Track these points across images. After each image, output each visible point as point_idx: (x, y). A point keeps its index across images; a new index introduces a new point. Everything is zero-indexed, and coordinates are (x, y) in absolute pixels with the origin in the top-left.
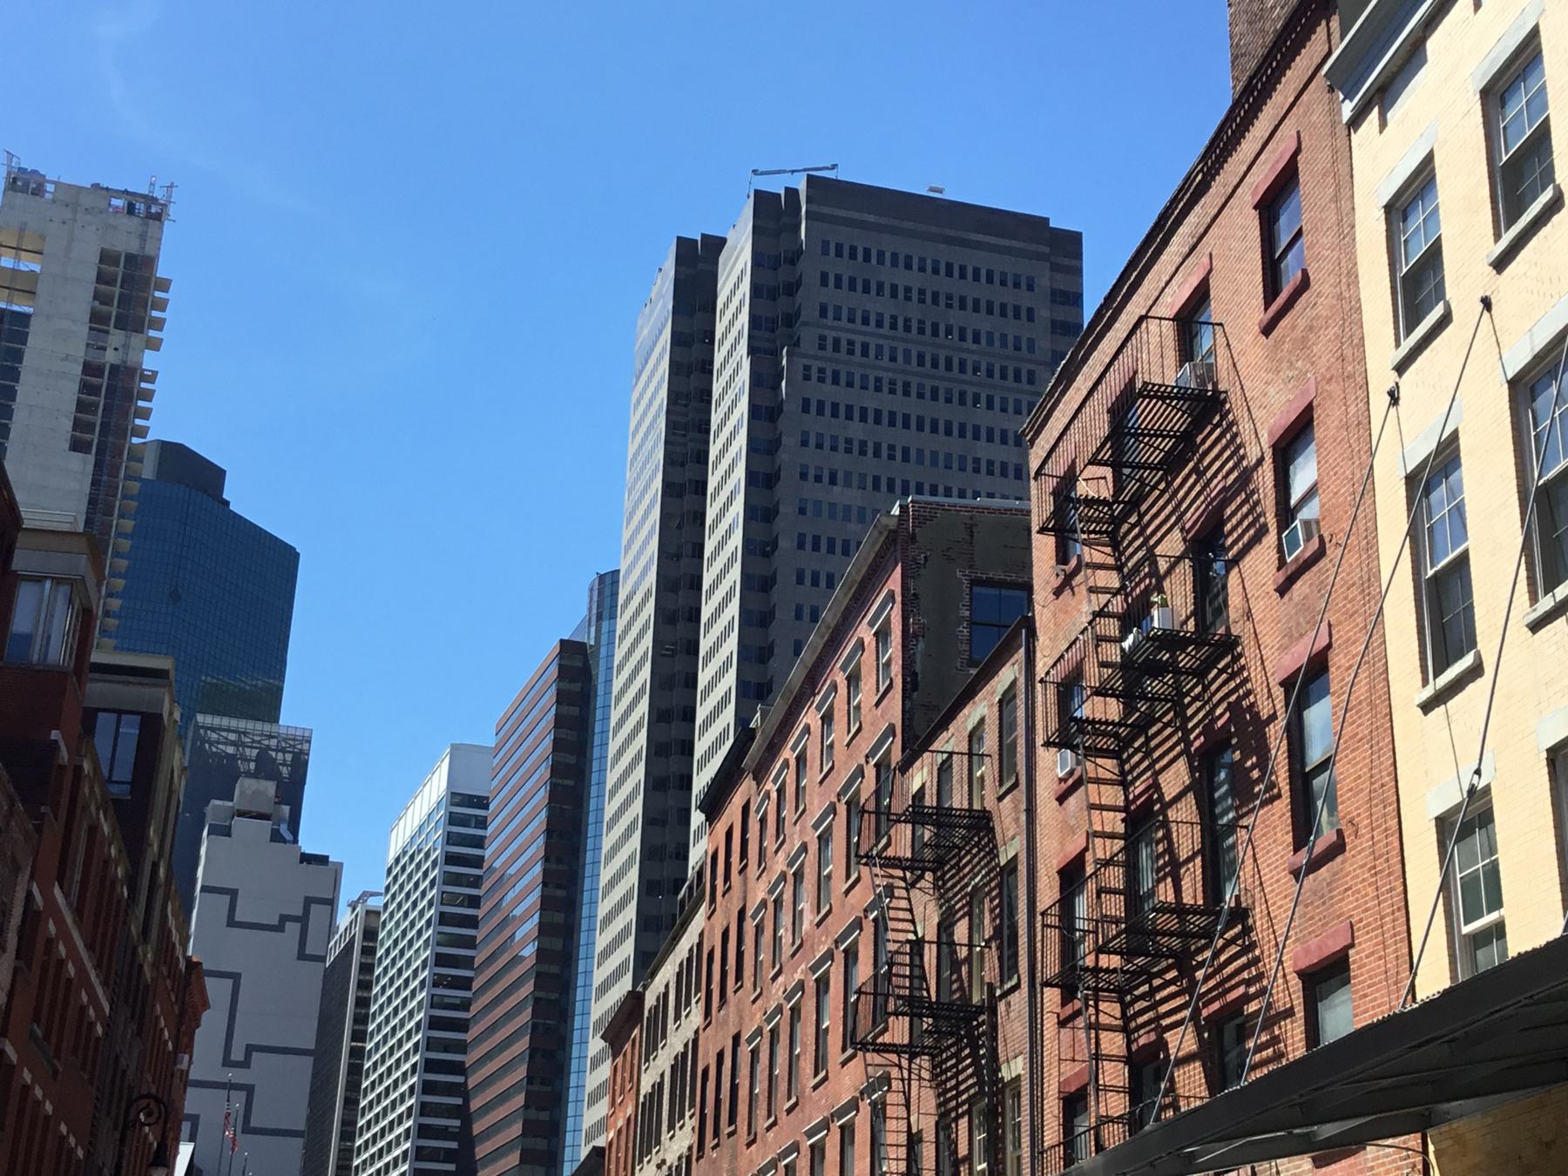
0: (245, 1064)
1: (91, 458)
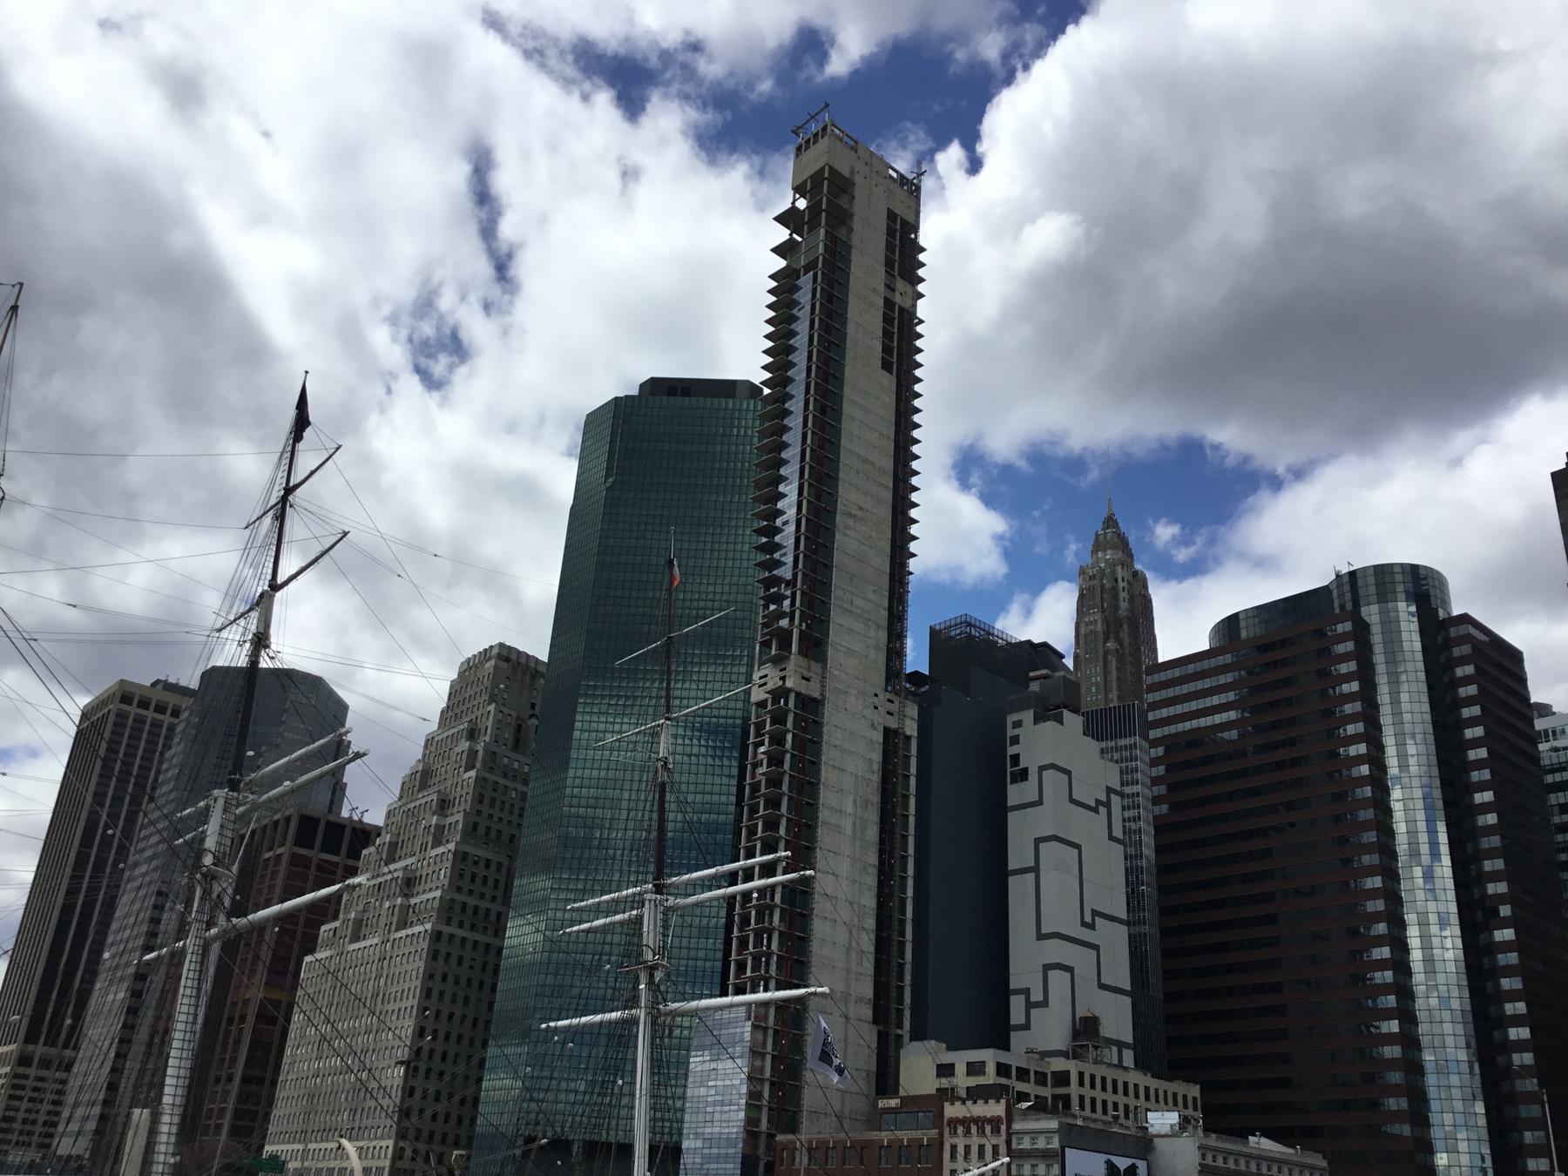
0: (1092, 926)
1: (895, 380)
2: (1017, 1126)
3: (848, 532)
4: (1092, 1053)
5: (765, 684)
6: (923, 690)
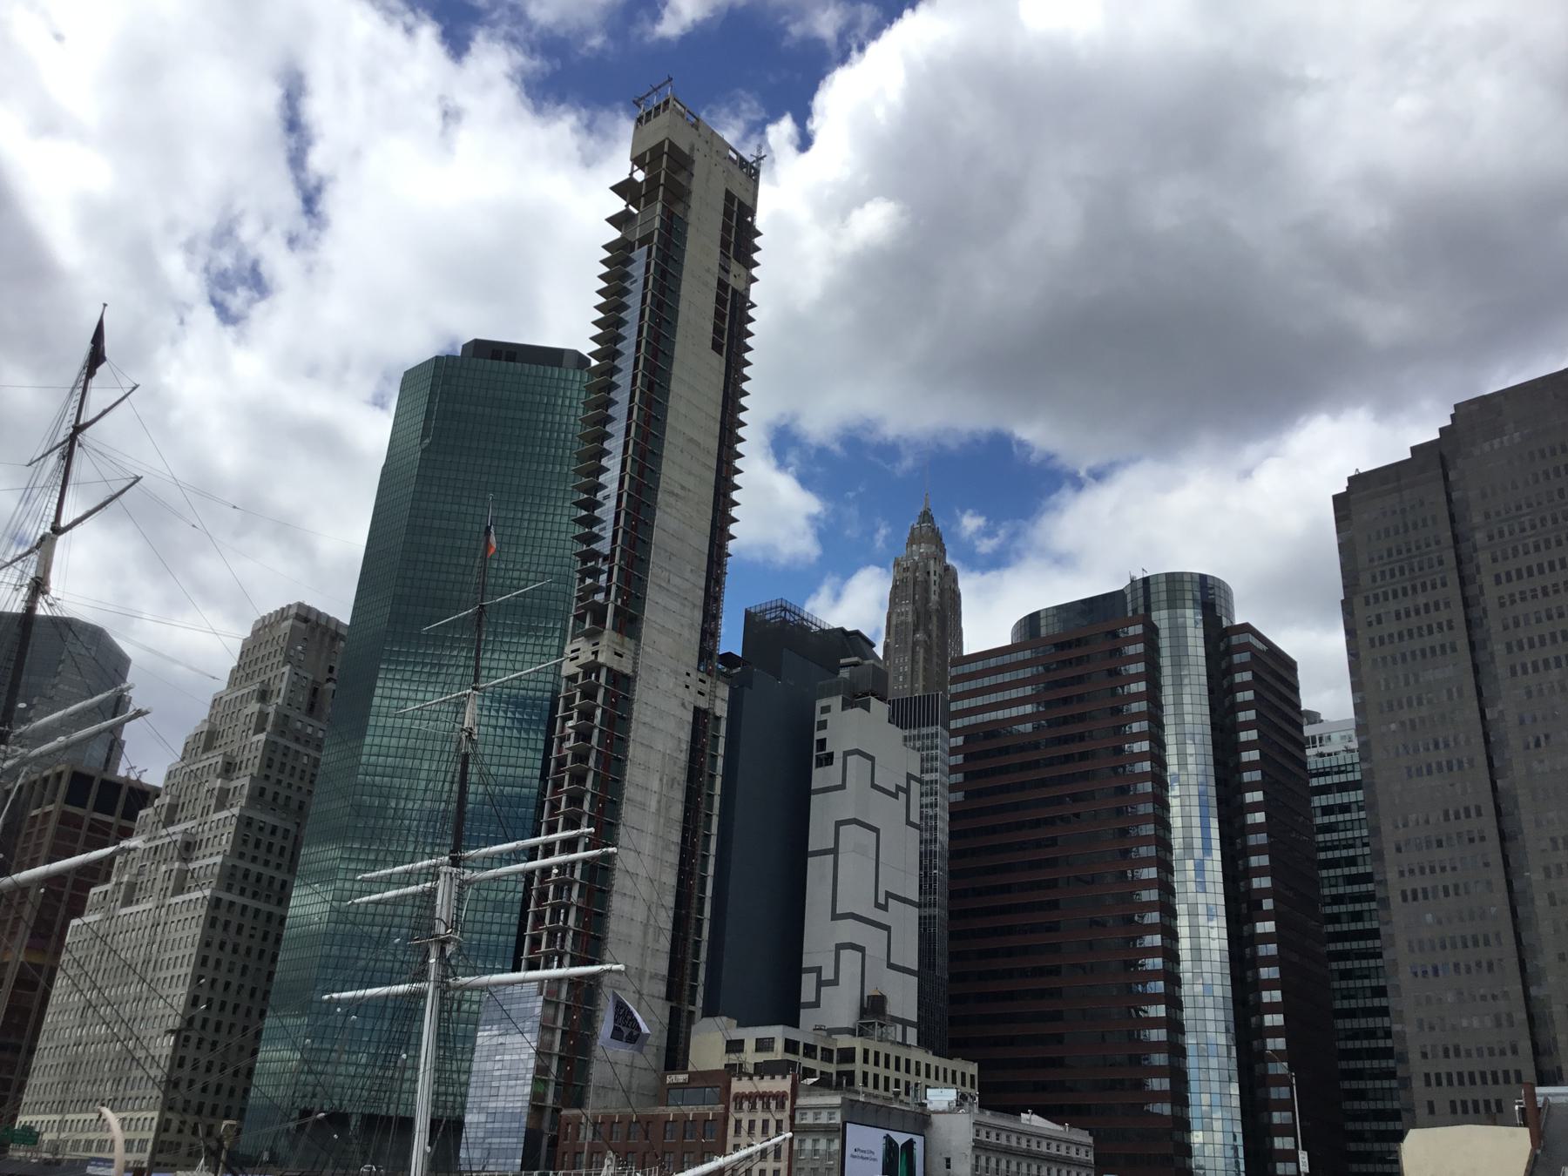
0: (885, 908)
1: (724, 360)
2: (801, 1102)
3: (668, 510)
4: (877, 1031)
5: (577, 658)
6: (734, 671)
